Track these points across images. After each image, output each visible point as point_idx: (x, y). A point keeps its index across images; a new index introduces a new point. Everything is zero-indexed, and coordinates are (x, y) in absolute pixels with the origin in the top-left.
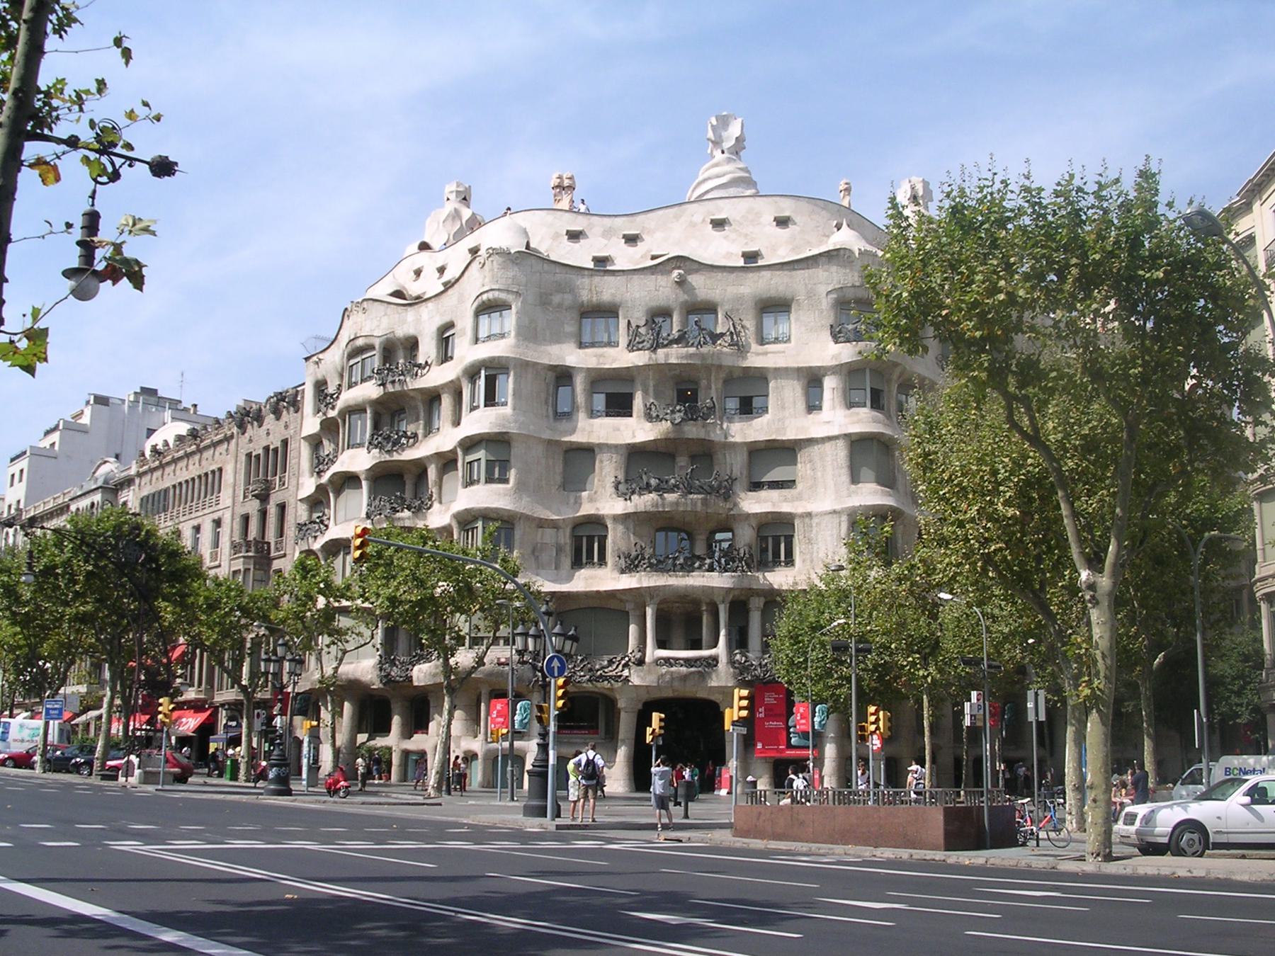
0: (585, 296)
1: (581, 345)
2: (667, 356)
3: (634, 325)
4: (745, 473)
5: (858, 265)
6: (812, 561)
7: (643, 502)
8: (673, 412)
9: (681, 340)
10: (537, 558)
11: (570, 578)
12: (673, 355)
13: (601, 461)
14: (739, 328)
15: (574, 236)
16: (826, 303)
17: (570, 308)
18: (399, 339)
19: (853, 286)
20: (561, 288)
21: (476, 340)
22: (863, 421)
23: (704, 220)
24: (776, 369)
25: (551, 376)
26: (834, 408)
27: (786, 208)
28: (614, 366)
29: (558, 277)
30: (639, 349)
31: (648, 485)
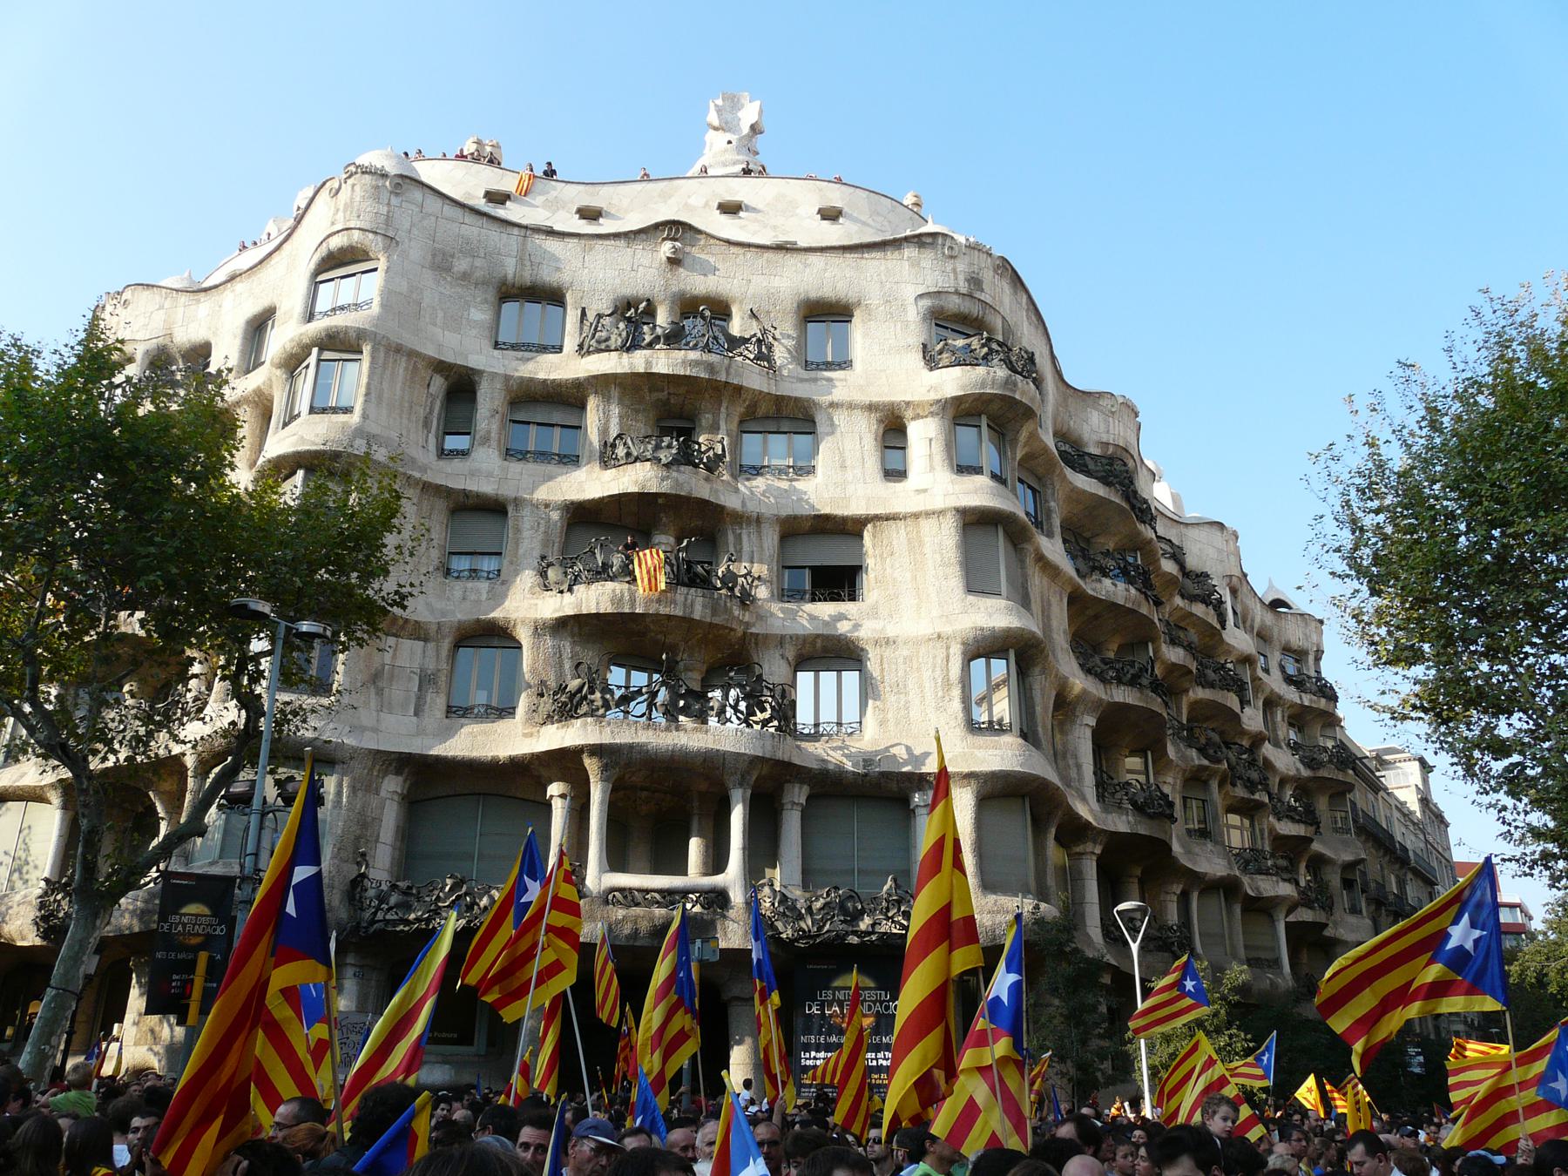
0: (510, 268)
1: (496, 345)
2: (648, 363)
3: (591, 316)
5: (961, 266)
6: (897, 724)
7: (594, 598)
8: (657, 447)
9: (674, 338)
11: (447, 734)
12: (664, 362)
13: (518, 530)
16: (913, 314)
17: (484, 283)
19: (957, 293)
21: (310, 316)
22: (978, 492)
23: (706, 205)
24: (832, 405)
25: (439, 384)
27: (836, 197)
30: (599, 351)
31: (606, 566)
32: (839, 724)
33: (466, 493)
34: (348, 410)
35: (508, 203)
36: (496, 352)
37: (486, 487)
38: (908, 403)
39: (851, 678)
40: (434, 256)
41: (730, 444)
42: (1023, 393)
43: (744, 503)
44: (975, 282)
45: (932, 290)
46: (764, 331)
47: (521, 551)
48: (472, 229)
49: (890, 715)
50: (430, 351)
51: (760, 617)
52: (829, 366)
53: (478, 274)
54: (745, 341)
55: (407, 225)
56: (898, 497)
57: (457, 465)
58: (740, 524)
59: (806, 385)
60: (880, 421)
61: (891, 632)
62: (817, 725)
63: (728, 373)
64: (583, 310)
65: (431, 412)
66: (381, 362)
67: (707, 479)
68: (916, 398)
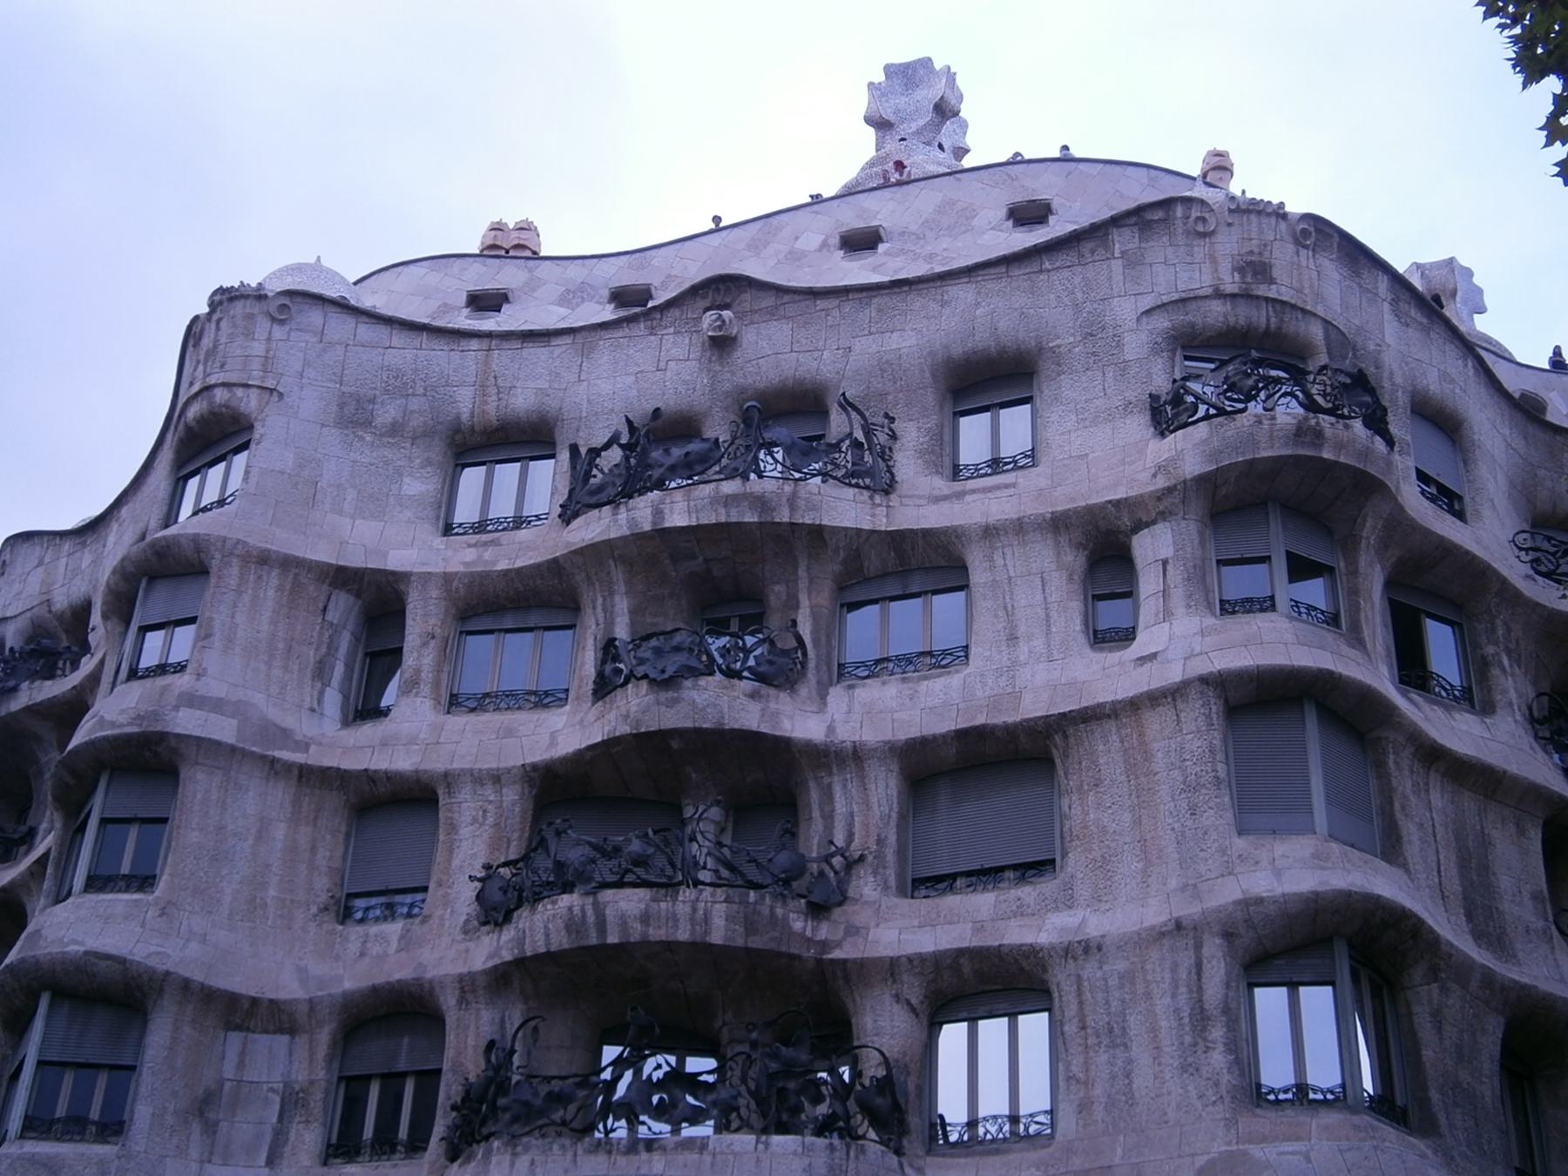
0: (464, 403)
1: (448, 530)
2: (658, 513)
4: (892, 839)
5: (1228, 245)
10: (210, 1129)
12: (679, 508)
13: (453, 828)
14: (881, 438)
16: (1136, 343)
18: (60, 617)
19: (1218, 294)
20: (400, 387)
24: (990, 532)
25: (342, 607)
26: (1167, 614)
28: (519, 564)
29: (394, 358)
32: (1014, 1119)
33: (369, 776)
34: (180, 668)
35: (505, 308)
36: (439, 542)
37: (402, 762)
38: (1117, 504)
39: (1034, 1026)
40: (342, 406)
41: (815, 632)
42: (1339, 446)
43: (831, 729)
44: (1256, 268)
45: (1165, 299)
46: (868, 432)
47: (456, 863)
48: (404, 352)
49: (1098, 1091)
50: (323, 554)
51: (852, 931)
52: (996, 465)
53: (416, 422)
54: (836, 447)
55: (298, 366)
56: (1108, 677)
57: (368, 731)
58: (828, 767)
59: (946, 505)
60: (1080, 546)
61: (1096, 924)
62: (972, 1124)
63: (793, 508)
64: (574, 449)
65: (332, 648)
66: (233, 582)
67: (753, 695)
68: (1132, 493)
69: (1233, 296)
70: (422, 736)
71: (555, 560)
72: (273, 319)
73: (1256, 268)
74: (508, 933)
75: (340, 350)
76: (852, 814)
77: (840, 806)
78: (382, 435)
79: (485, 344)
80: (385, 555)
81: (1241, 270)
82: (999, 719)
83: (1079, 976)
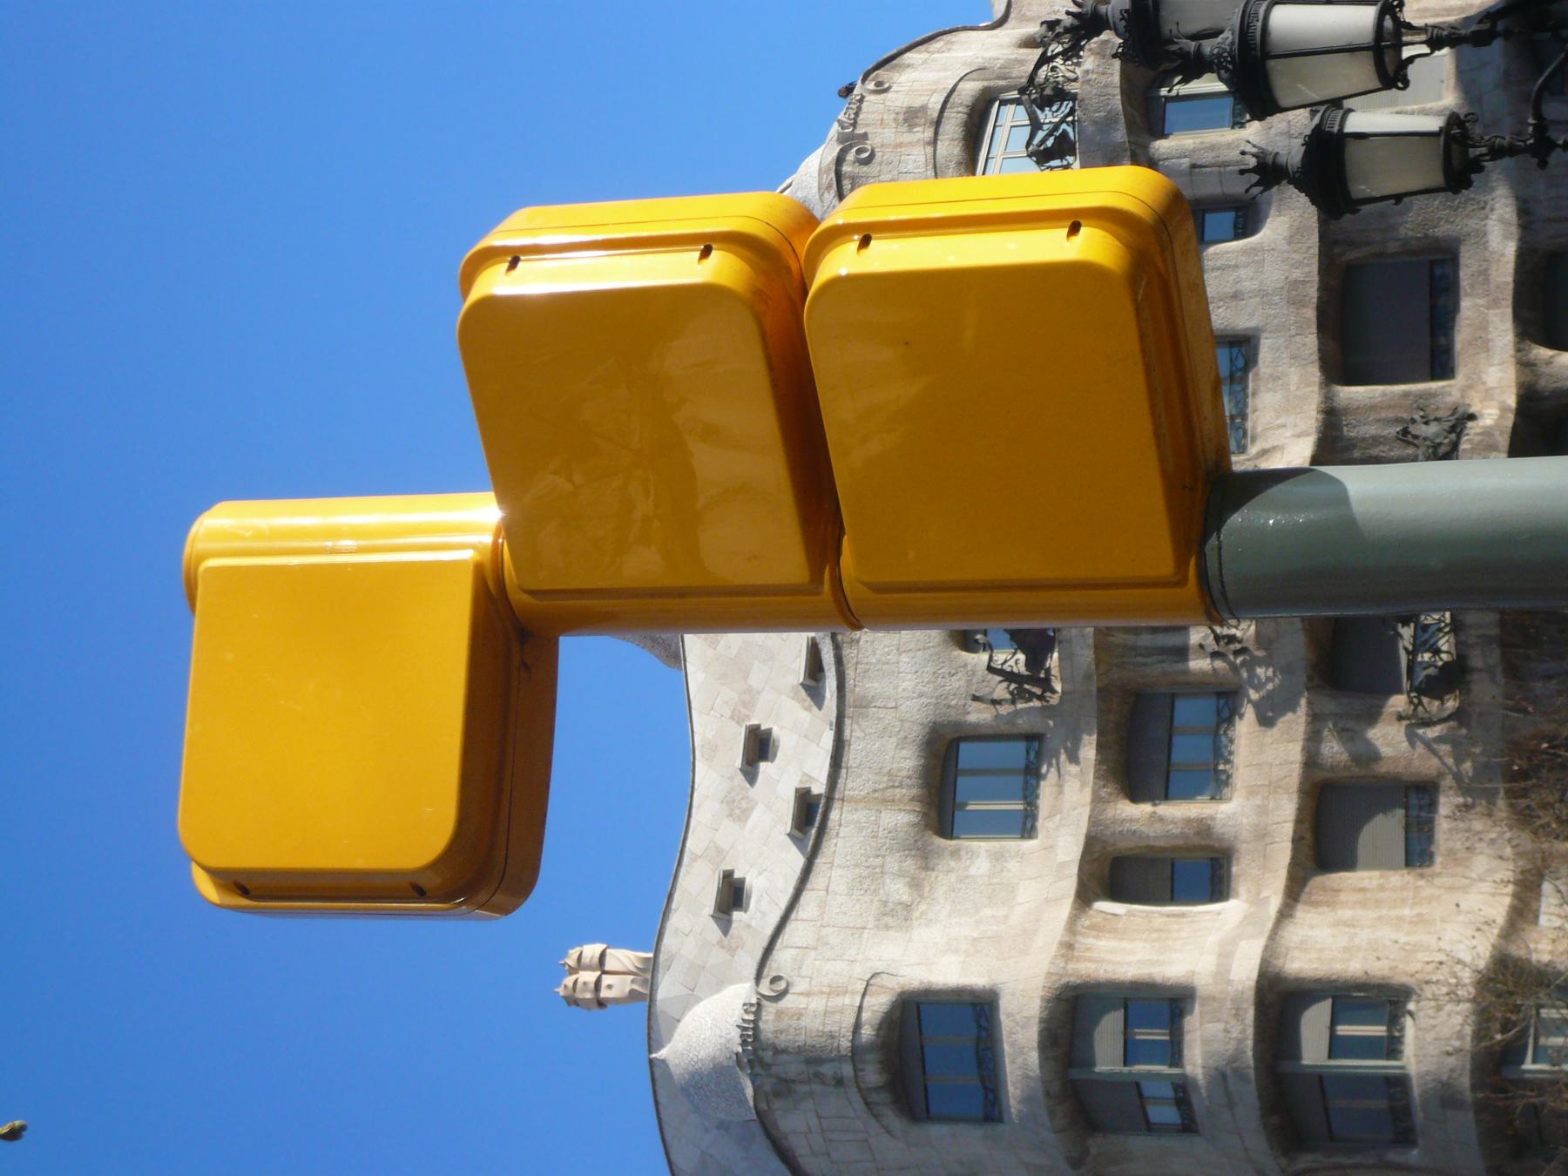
15: (732, 895)
33: (1297, 840)
35: (737, 875)
37: (1285, 811)
40: (887, 927)
53: (910, 864)
69: (936, 133)
70: (1258, 802)
71: (1099, 690)
72: (784, 993)
73: (911, 117)
74: (1476, 660)
75: (825, 931)
76: (1378, 421)
77: (1372, 430)
78: (921, 896)
79: (837, 805)
80: (1063, 865)
81: (911, 126)
82: (1312, 292)
83: (1550, 220)
